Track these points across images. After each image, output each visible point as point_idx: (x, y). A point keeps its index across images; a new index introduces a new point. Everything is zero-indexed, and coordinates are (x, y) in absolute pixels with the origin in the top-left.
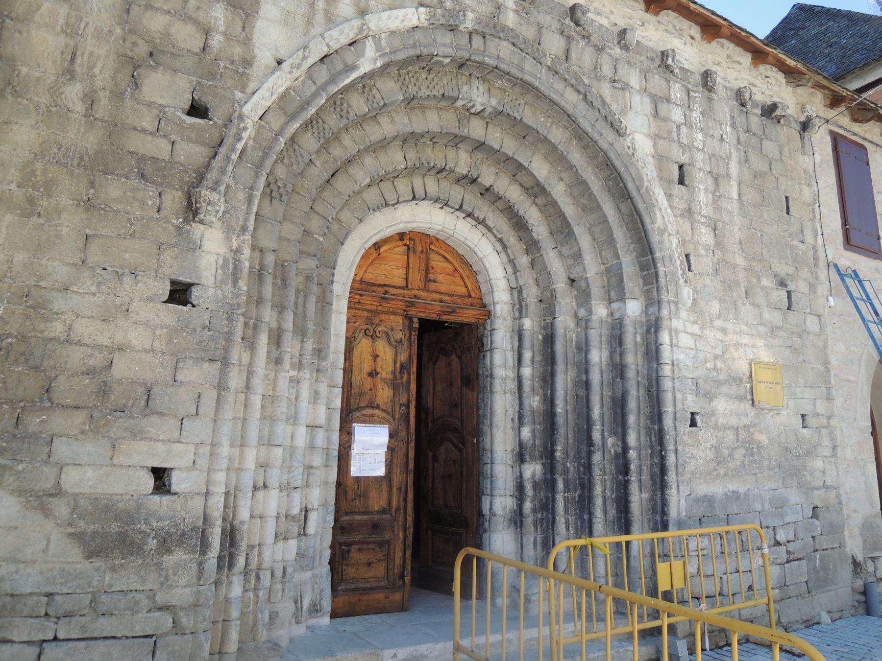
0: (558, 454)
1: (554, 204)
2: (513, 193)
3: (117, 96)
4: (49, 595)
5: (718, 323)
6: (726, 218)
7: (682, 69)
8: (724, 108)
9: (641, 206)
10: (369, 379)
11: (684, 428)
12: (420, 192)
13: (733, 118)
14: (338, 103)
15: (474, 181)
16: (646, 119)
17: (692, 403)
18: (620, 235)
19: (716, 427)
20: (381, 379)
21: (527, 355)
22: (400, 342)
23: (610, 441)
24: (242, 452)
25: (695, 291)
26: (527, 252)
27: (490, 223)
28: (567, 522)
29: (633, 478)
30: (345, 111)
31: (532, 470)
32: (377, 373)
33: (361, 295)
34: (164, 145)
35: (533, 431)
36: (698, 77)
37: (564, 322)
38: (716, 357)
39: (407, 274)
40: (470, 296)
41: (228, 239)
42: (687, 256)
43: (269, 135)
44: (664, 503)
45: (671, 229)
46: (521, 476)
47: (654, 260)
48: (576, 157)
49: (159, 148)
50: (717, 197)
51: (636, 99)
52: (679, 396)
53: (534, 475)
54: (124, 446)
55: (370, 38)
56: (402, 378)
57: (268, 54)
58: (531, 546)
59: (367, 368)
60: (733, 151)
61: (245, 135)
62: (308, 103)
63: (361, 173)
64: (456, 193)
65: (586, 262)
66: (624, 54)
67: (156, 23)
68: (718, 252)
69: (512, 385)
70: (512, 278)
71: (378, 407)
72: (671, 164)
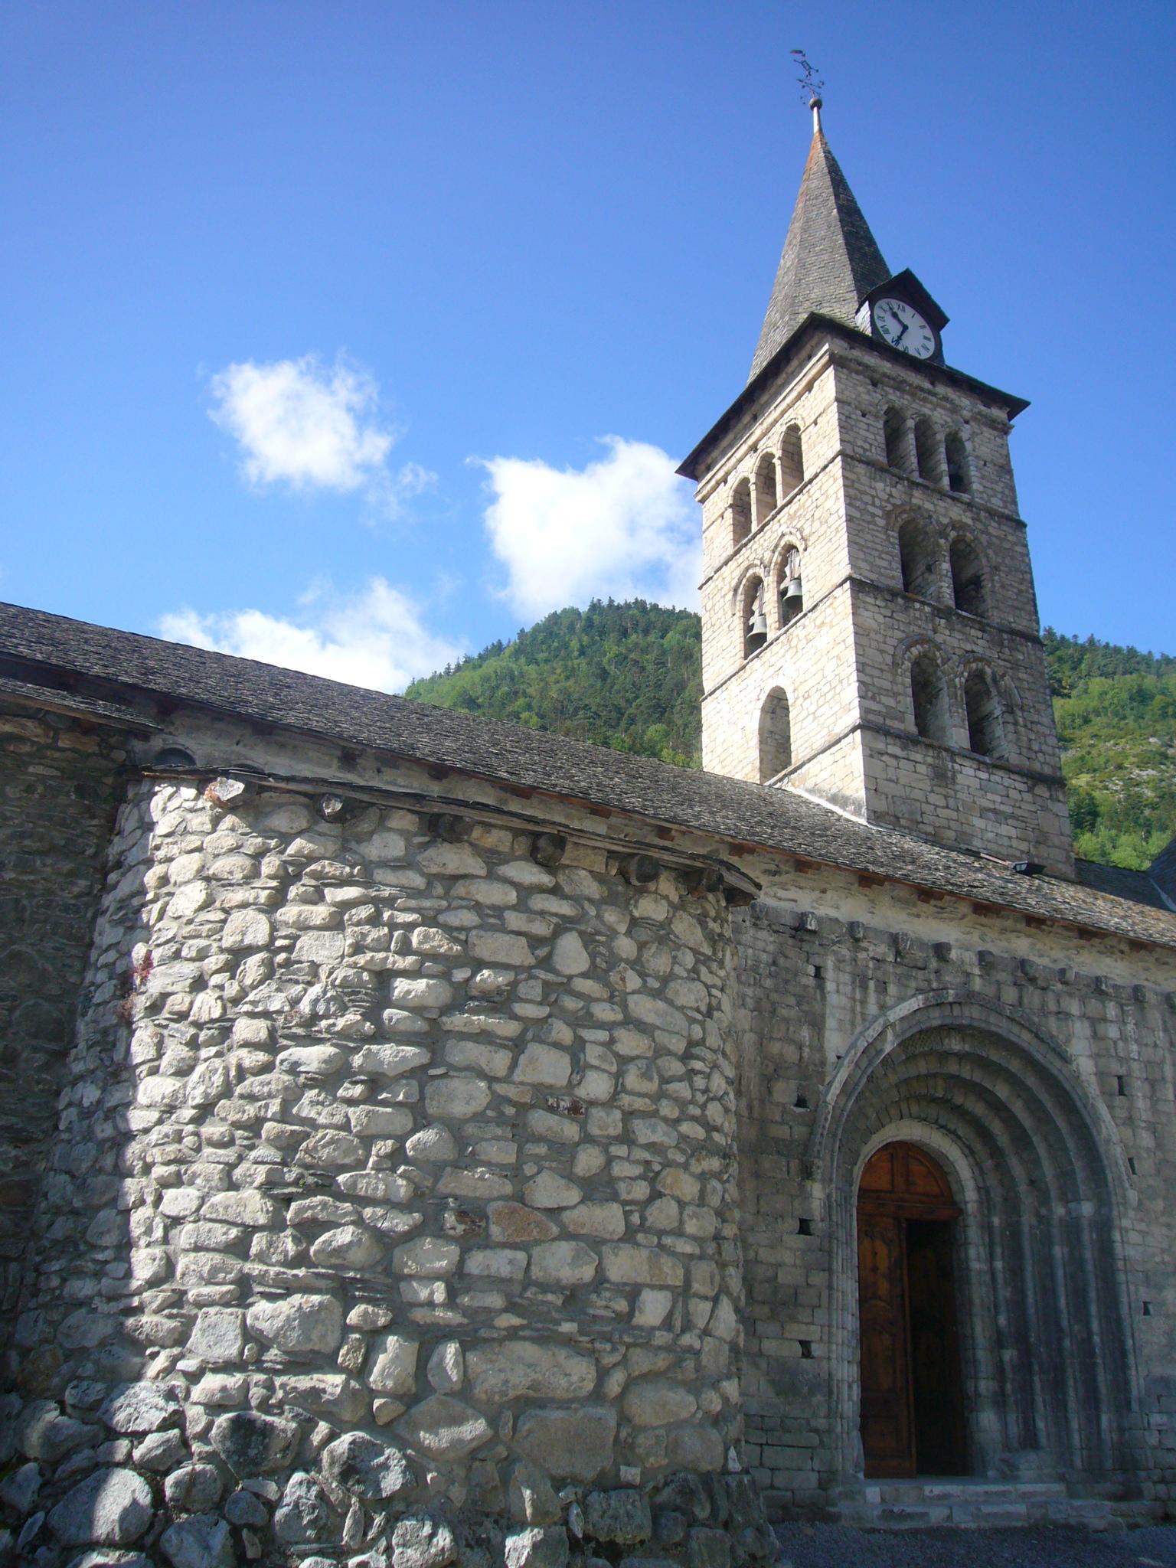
0: (1032, 1340)
1: (1015, 1117)
2: (979, 1109)
3: (762, 1101)
4: (762, 1417)
5: (1163, 1219)
6: (1164, 1119)
7: (1115, 986)
8: (1155, 1017)
9: (1089, 1121)
11: (1139, 1317)
12: (905, 1111)
13: (1164, 1022)
15: (948, 1101)
17: (1144, 1293)
19: (1167, 1316)
21: (998, 1250)
23: (1076, 1327)
25: (1140, 1192)
26: (992, 1156)
27: (960, 1133)
28: (1044, 1401)
34: (786, 1127)
35: (1008, 1319)
36: (1129, 990)
37: (1027, 1220)
38: (1163, 1251)
41: (824, 1188)
42: (1130, 1160)
44: (1127, 1382)
45: (1115, 1139)
46: (1001, 1360)
48: (1031, 1081)
49: (782, 1132)
50: (1153, 1098)
52: (1132, 1288)
54: (787, 1327)
60: (1167, 1055)
62: (857, 1084)
64: (932, 1111)
67: (775, 1048)
68: (1159, 1153)
69: (987, 1278)
70: (980, 1179)
71: (880, 1298)
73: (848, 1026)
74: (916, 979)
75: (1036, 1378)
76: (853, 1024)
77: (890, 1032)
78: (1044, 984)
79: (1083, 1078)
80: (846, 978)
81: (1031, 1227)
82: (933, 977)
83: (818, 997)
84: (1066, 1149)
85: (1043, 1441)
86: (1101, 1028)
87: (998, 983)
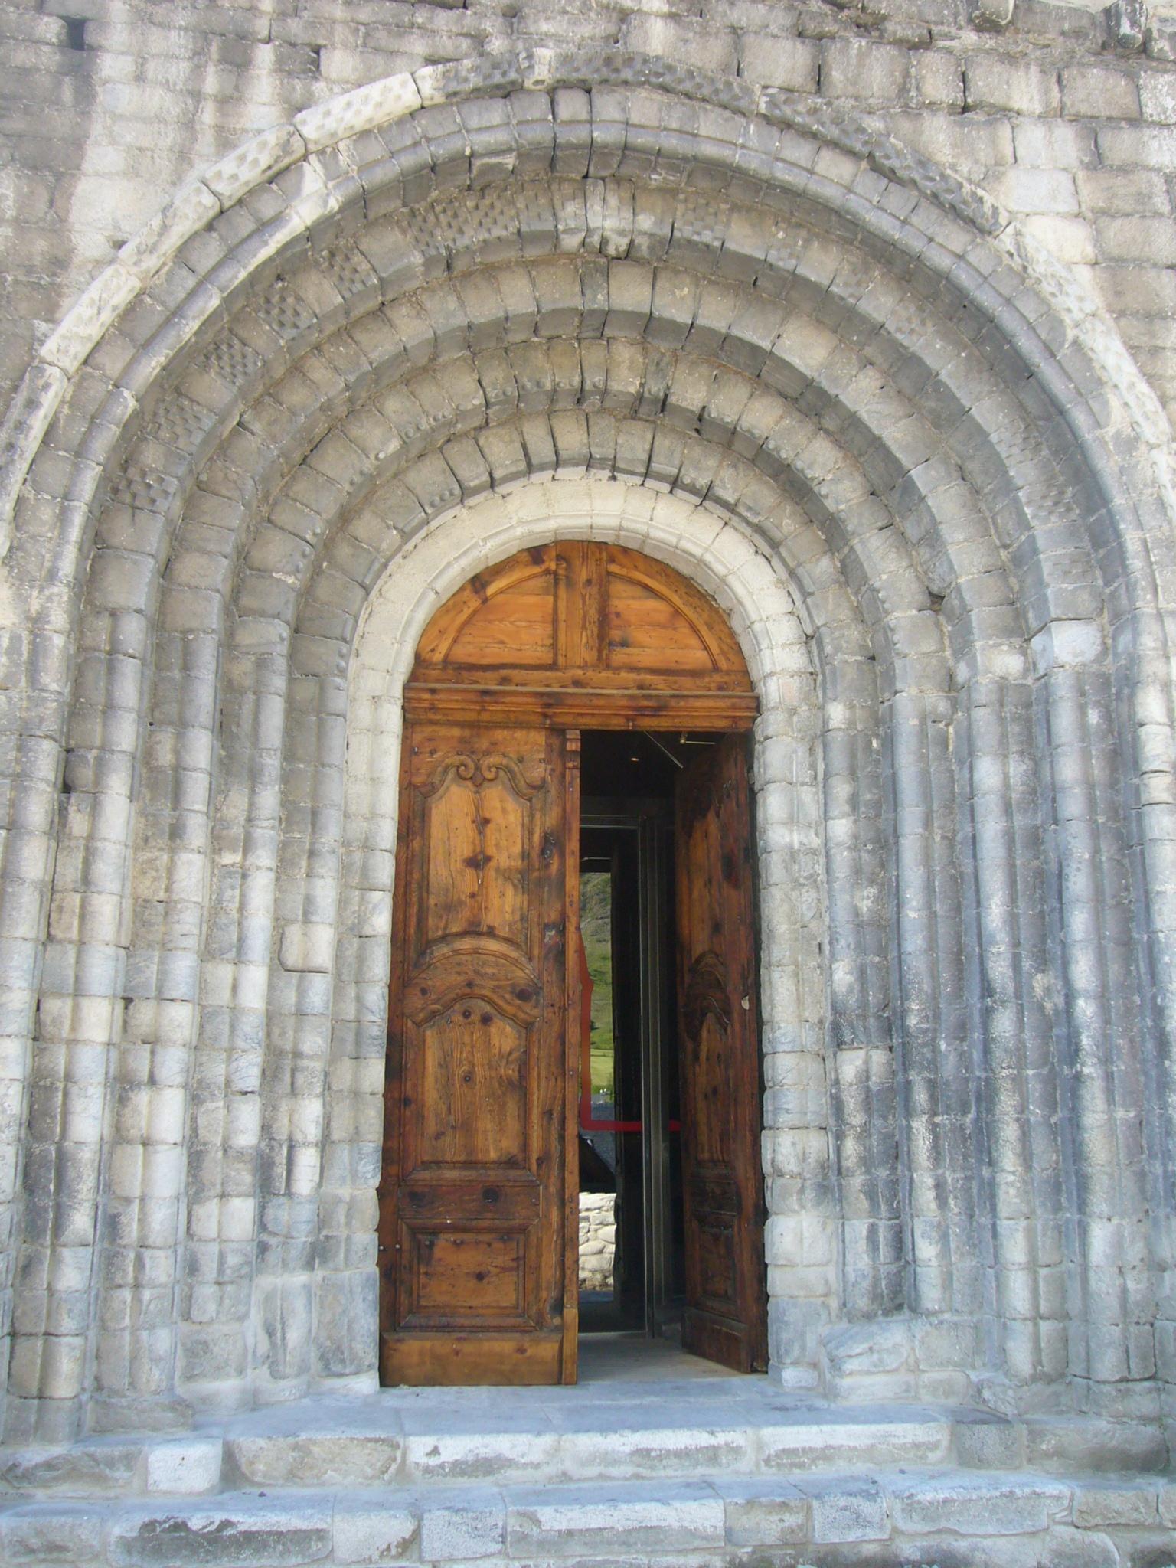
0: (912, 1021)
10: (470, 873)
12: (542, 450)
14: (276, 299)
16: (1065, 180)
18: (1024, 471)
20: (497, 870)
22: (541, 787)
24: (76, 1009)
28: (939, 1186)
29: (1090, 1068)
30: (289, 312)
31: (859, 1062)
32: (488, 859)
33: (433, 691)
35: (862, 973)
39: (555, 636)
40: (716, 668)
41: (21, 599)
43: (98, 390)
47: (1111, 514)
51: (1033, 138)
53: (865, 1076)
55: (312, 158)
56: (547, 866)
57: (100, 238)
58: (862, 1245)
59: (463, 847)
61: (49, 402)
62: (177, 313)
63: (378, 432)
64: (633, 443)
65: (952, 550)
66: (990, 41)
71: (491, 933)
72: (1153, 273)
73: (165, 164)
74: (426, 31)
75: (920, 1125)
76: (183, 157)
77: (313, 177)
78: (912, 34)
79: (1038, 269)
80: (178, 41)
81: (925, 718)
82: (491, 25)
83: (67, 94)
84: (1008, 487)
85: (931, 1294)
86: (1120, 144)
87: (735, 31)
